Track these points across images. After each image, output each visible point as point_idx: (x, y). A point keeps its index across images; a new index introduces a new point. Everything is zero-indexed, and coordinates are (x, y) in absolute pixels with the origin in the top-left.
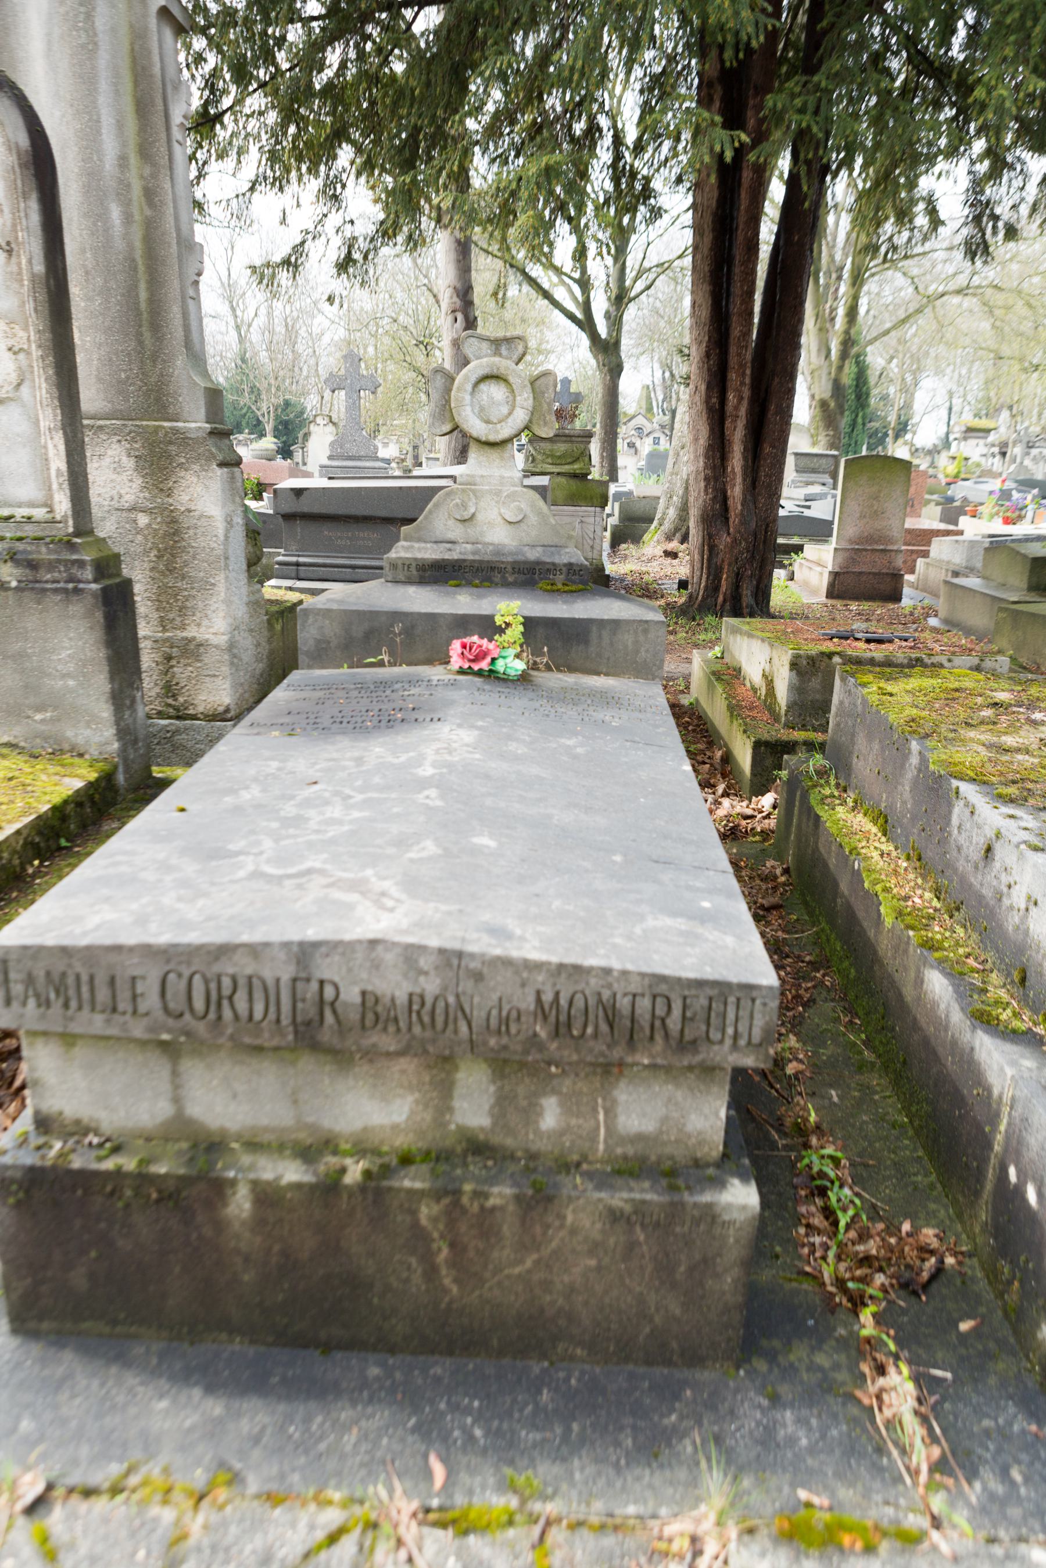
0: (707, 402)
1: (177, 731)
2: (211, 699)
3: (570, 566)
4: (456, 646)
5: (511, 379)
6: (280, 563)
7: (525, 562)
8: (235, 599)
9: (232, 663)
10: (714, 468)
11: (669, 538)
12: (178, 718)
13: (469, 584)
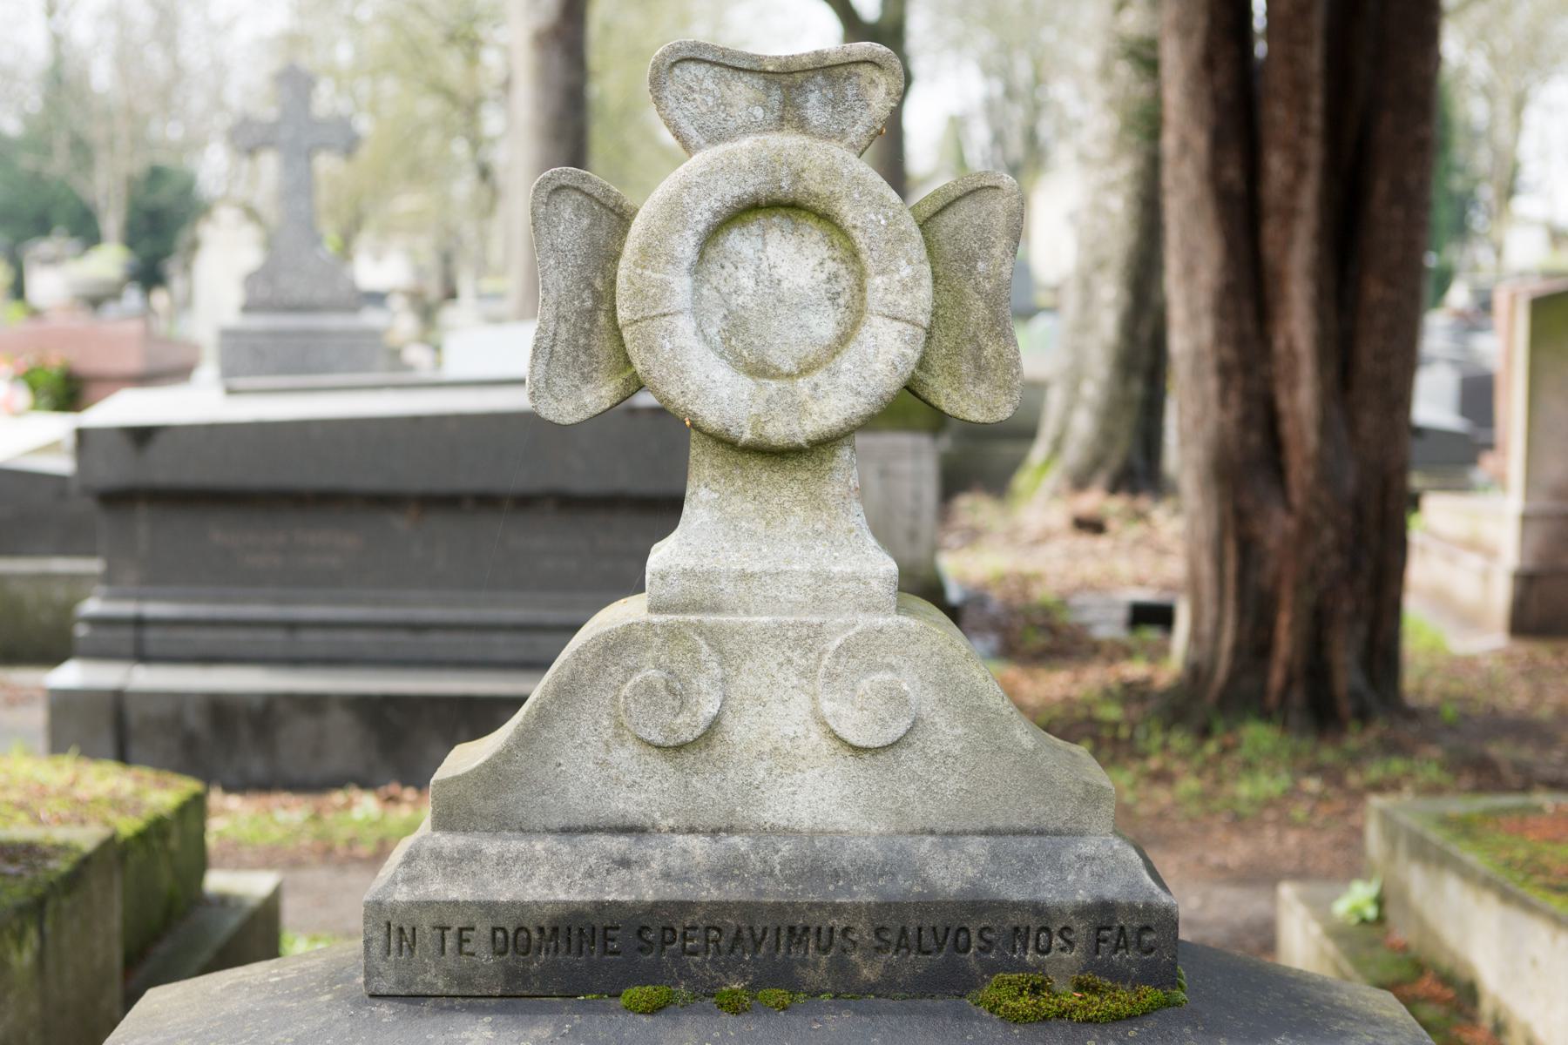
0: (1214, 175)
3: (1102, 914)
5: (848, 213)
6: (98, 622)
7: (926, 906)
10: (1240, 342)
11: (1080, 482)
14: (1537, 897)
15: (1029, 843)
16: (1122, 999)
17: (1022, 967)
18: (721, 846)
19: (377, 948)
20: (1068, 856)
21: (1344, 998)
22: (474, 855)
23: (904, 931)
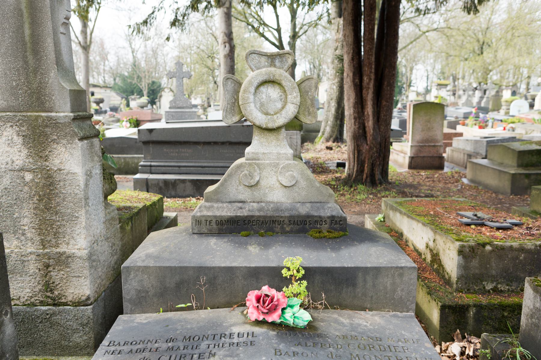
0: (354, 81)
1: (54, 314)
2: (77, 292)
3: (332, 218)
4: (252, 296)
5: (284, 83)
6: (142, 166)
7: (299, 216)
8: (95, 223)
9: (91, 267)
10: (358, 113)
11: (328, 141)
12: (54, 305)
13: (257, 233)
14: (414, 216)
15: (318, 204)
16: (336, 234)
17: (317, 228)
18: (259, 205)
19: (194, 224)
20: (326, 207)
21: (378, 234)
22: (212, 207)
23: (294, 221)
